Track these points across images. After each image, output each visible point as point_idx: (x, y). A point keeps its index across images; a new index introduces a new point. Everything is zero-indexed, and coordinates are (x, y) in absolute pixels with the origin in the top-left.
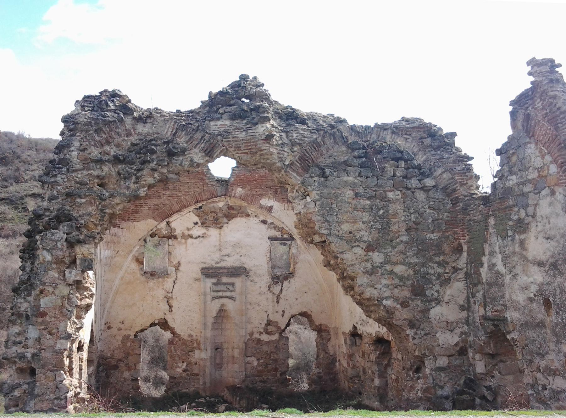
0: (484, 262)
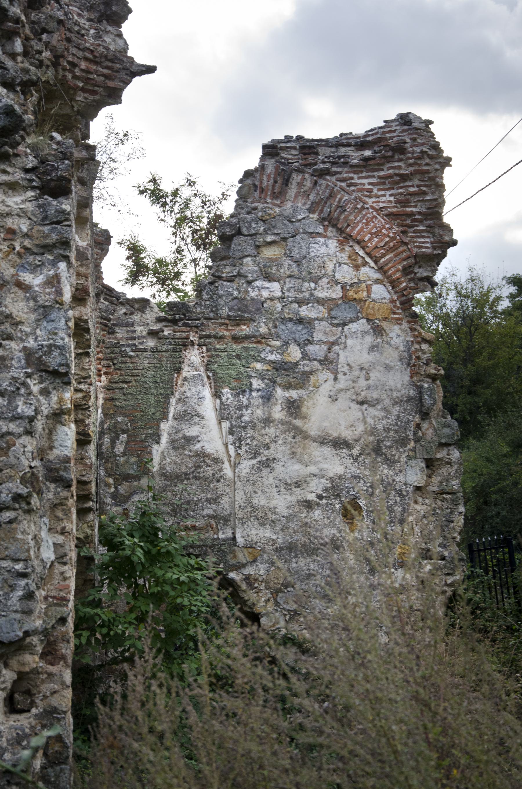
0: (162, 432)
